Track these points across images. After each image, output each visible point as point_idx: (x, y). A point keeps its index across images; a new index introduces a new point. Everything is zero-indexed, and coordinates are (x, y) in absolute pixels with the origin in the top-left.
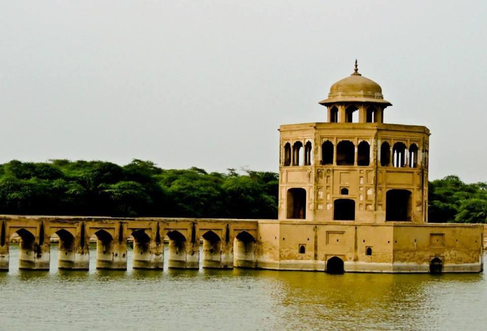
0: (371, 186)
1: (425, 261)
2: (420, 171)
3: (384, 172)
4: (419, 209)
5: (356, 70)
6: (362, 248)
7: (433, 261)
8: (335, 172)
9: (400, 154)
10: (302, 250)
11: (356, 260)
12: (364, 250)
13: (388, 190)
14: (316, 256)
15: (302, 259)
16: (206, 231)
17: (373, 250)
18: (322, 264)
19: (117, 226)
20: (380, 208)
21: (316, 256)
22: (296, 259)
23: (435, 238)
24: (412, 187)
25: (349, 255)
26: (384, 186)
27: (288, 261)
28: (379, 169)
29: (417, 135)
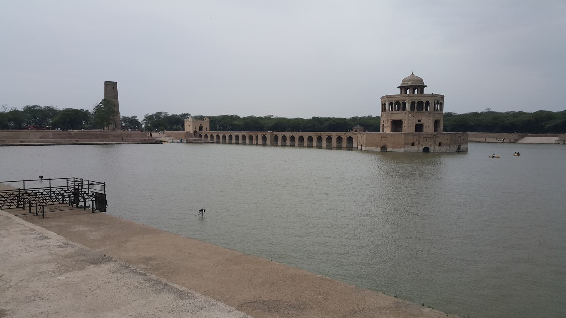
23: (383, 139)
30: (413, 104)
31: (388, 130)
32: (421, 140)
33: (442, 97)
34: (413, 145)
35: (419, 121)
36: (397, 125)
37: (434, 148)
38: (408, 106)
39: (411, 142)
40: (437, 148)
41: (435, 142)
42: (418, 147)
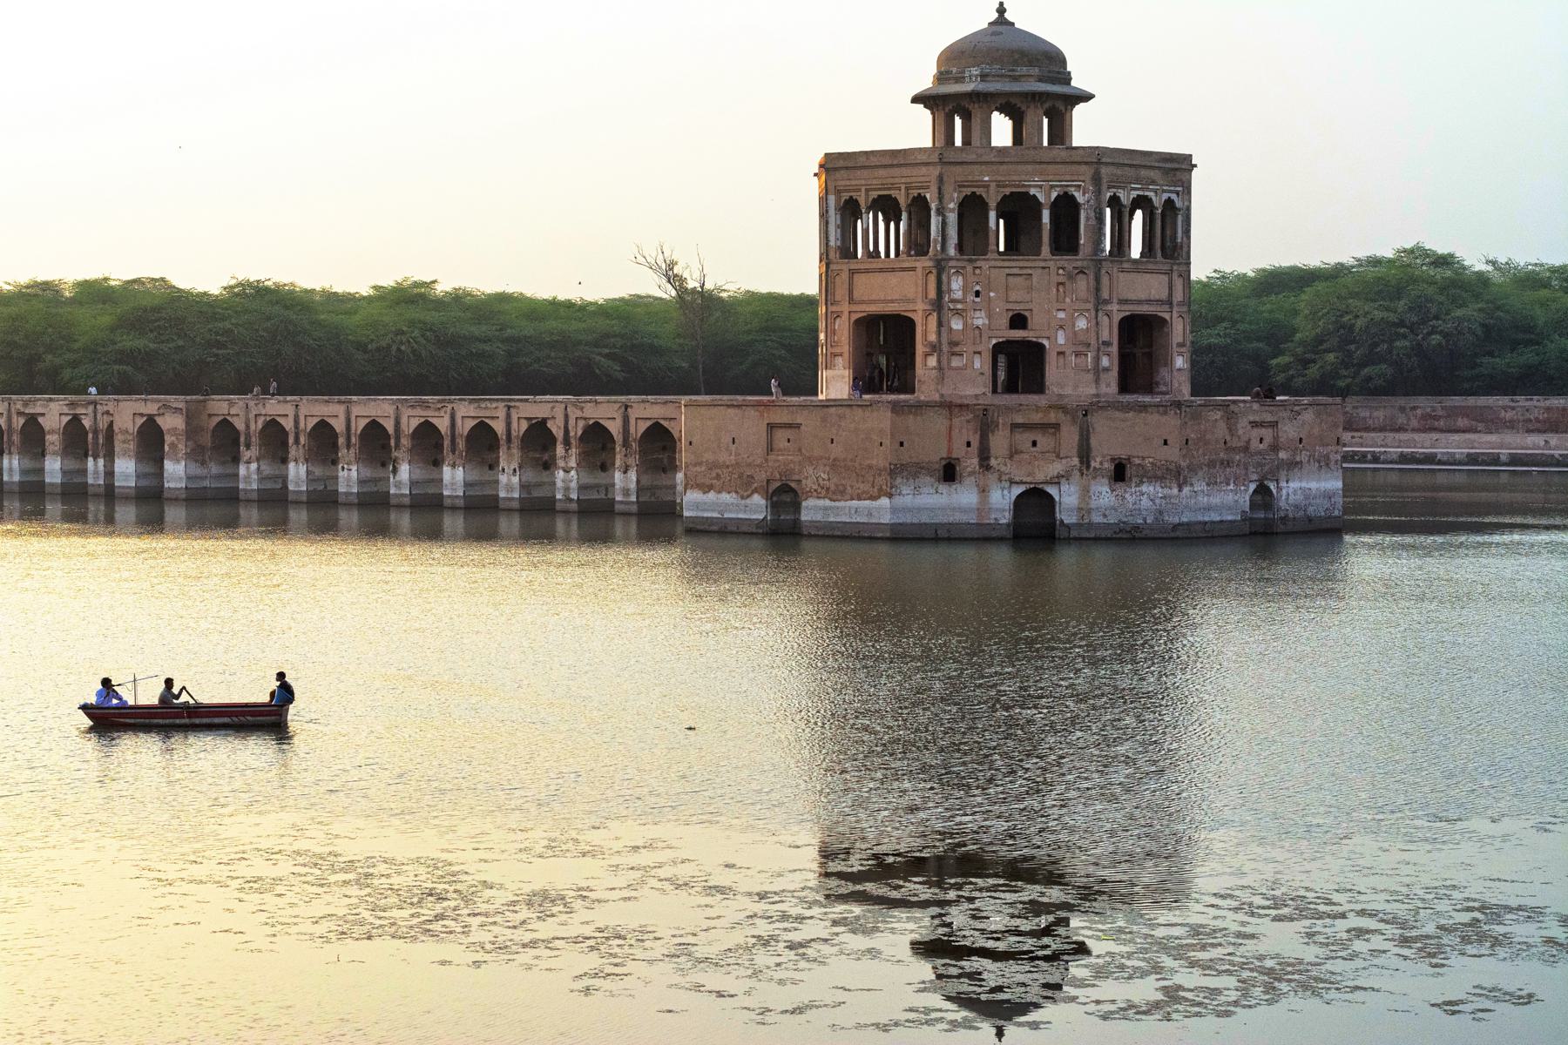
0: (1084, 306)
1: (755, 491)
2: (930, 264)
3: (845, 276)
4: (932, 361)
5: (1001, 10)
7: (777, 491)
9: (892, 225)
13: (855, 317)
16: (649, 423)
19: (501, 413)
20: (839, 360)
23: (781, 436)
24: (911, 307)
26: (845, 308)
28: (833, 267)
29: (924, 170)
30: (972, 208)
31: (835, 382)
32: (999, 442)
33: (1177, 168)
34: (949, 473)
35: (1018, 321)
36: (886, 350)
37: (1085, 493)
38: (944, 225)
39: (936, 453)
40: (1104, 495)
41: (1085, 455)
42: (983, 491)
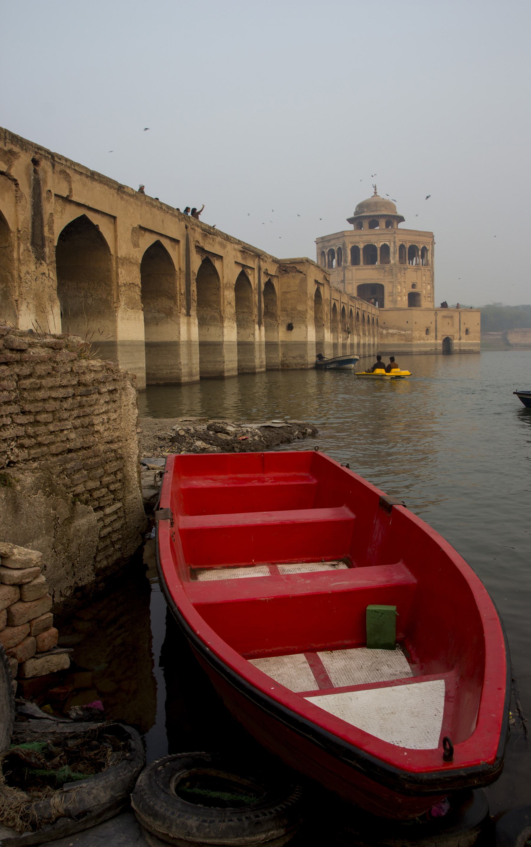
6: (463, 329)
8: (408, 270)
10: (427, 331)
11: (460, 339)
12: (465, 330)
14: (436, 336)
15: (428, 340)
17: (470, 330)
18: (440, 342)
21: (436, 336)
22: (424, 340)
25: (457, 336)
27: (419, 342)
